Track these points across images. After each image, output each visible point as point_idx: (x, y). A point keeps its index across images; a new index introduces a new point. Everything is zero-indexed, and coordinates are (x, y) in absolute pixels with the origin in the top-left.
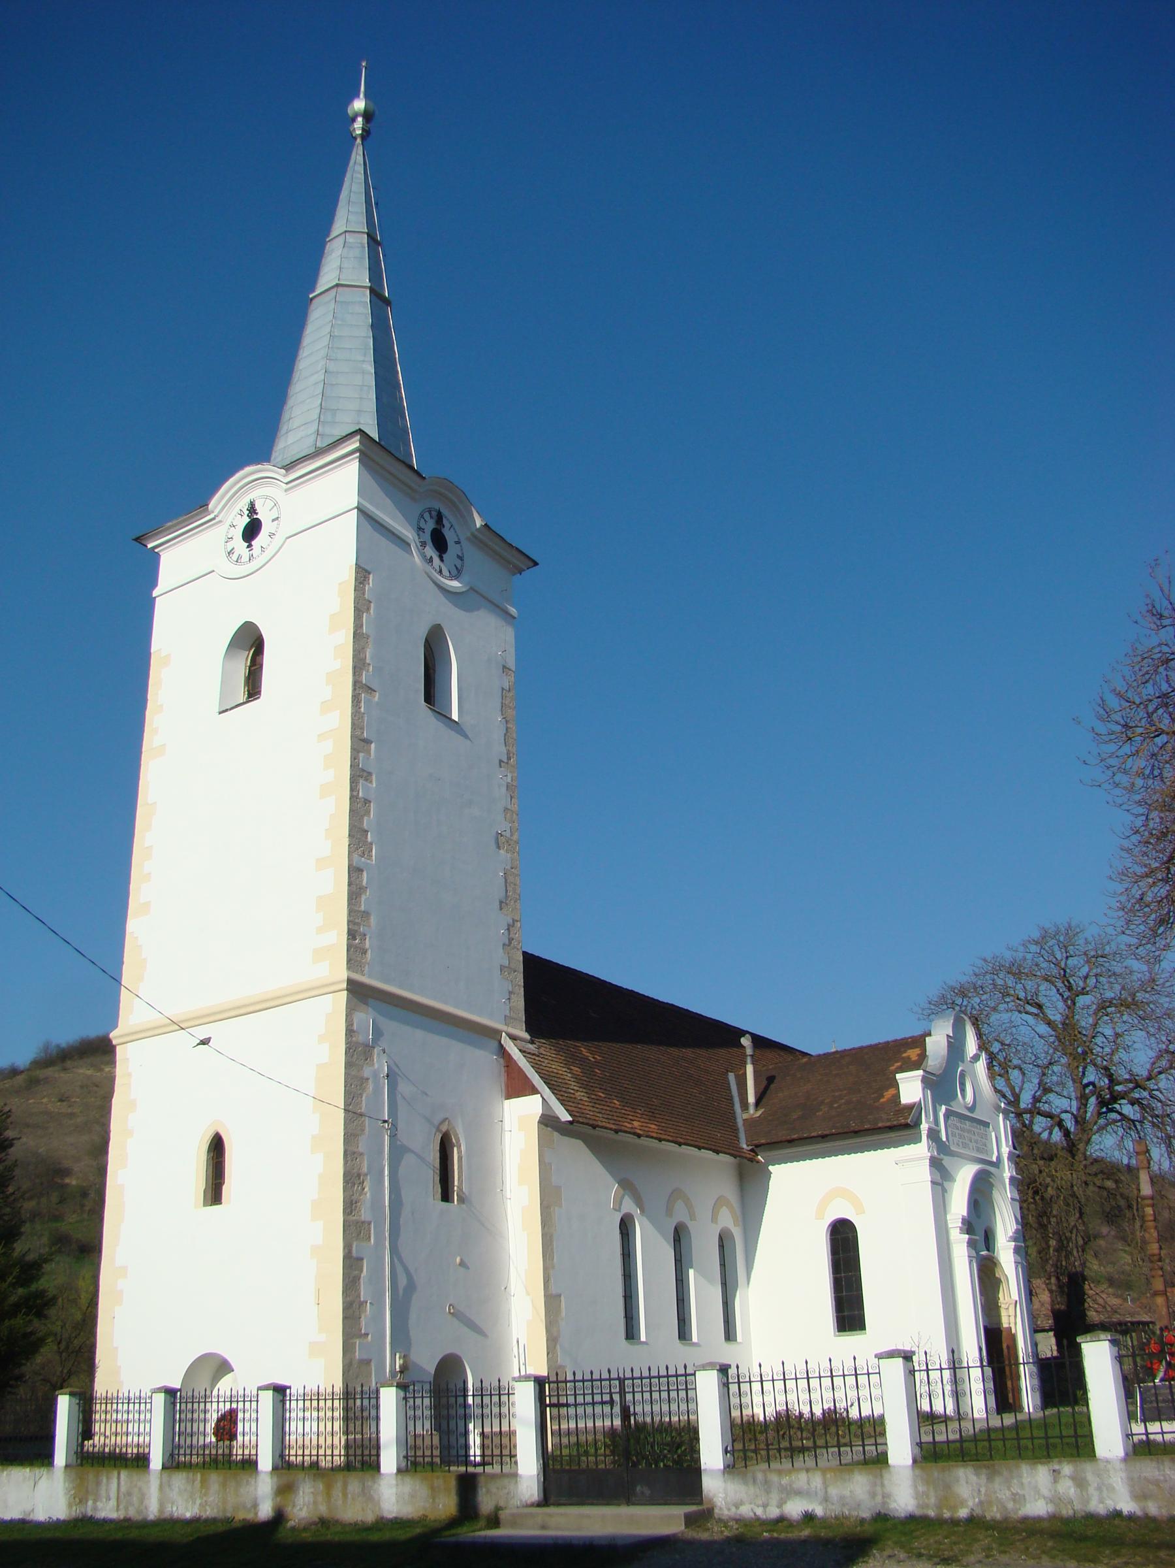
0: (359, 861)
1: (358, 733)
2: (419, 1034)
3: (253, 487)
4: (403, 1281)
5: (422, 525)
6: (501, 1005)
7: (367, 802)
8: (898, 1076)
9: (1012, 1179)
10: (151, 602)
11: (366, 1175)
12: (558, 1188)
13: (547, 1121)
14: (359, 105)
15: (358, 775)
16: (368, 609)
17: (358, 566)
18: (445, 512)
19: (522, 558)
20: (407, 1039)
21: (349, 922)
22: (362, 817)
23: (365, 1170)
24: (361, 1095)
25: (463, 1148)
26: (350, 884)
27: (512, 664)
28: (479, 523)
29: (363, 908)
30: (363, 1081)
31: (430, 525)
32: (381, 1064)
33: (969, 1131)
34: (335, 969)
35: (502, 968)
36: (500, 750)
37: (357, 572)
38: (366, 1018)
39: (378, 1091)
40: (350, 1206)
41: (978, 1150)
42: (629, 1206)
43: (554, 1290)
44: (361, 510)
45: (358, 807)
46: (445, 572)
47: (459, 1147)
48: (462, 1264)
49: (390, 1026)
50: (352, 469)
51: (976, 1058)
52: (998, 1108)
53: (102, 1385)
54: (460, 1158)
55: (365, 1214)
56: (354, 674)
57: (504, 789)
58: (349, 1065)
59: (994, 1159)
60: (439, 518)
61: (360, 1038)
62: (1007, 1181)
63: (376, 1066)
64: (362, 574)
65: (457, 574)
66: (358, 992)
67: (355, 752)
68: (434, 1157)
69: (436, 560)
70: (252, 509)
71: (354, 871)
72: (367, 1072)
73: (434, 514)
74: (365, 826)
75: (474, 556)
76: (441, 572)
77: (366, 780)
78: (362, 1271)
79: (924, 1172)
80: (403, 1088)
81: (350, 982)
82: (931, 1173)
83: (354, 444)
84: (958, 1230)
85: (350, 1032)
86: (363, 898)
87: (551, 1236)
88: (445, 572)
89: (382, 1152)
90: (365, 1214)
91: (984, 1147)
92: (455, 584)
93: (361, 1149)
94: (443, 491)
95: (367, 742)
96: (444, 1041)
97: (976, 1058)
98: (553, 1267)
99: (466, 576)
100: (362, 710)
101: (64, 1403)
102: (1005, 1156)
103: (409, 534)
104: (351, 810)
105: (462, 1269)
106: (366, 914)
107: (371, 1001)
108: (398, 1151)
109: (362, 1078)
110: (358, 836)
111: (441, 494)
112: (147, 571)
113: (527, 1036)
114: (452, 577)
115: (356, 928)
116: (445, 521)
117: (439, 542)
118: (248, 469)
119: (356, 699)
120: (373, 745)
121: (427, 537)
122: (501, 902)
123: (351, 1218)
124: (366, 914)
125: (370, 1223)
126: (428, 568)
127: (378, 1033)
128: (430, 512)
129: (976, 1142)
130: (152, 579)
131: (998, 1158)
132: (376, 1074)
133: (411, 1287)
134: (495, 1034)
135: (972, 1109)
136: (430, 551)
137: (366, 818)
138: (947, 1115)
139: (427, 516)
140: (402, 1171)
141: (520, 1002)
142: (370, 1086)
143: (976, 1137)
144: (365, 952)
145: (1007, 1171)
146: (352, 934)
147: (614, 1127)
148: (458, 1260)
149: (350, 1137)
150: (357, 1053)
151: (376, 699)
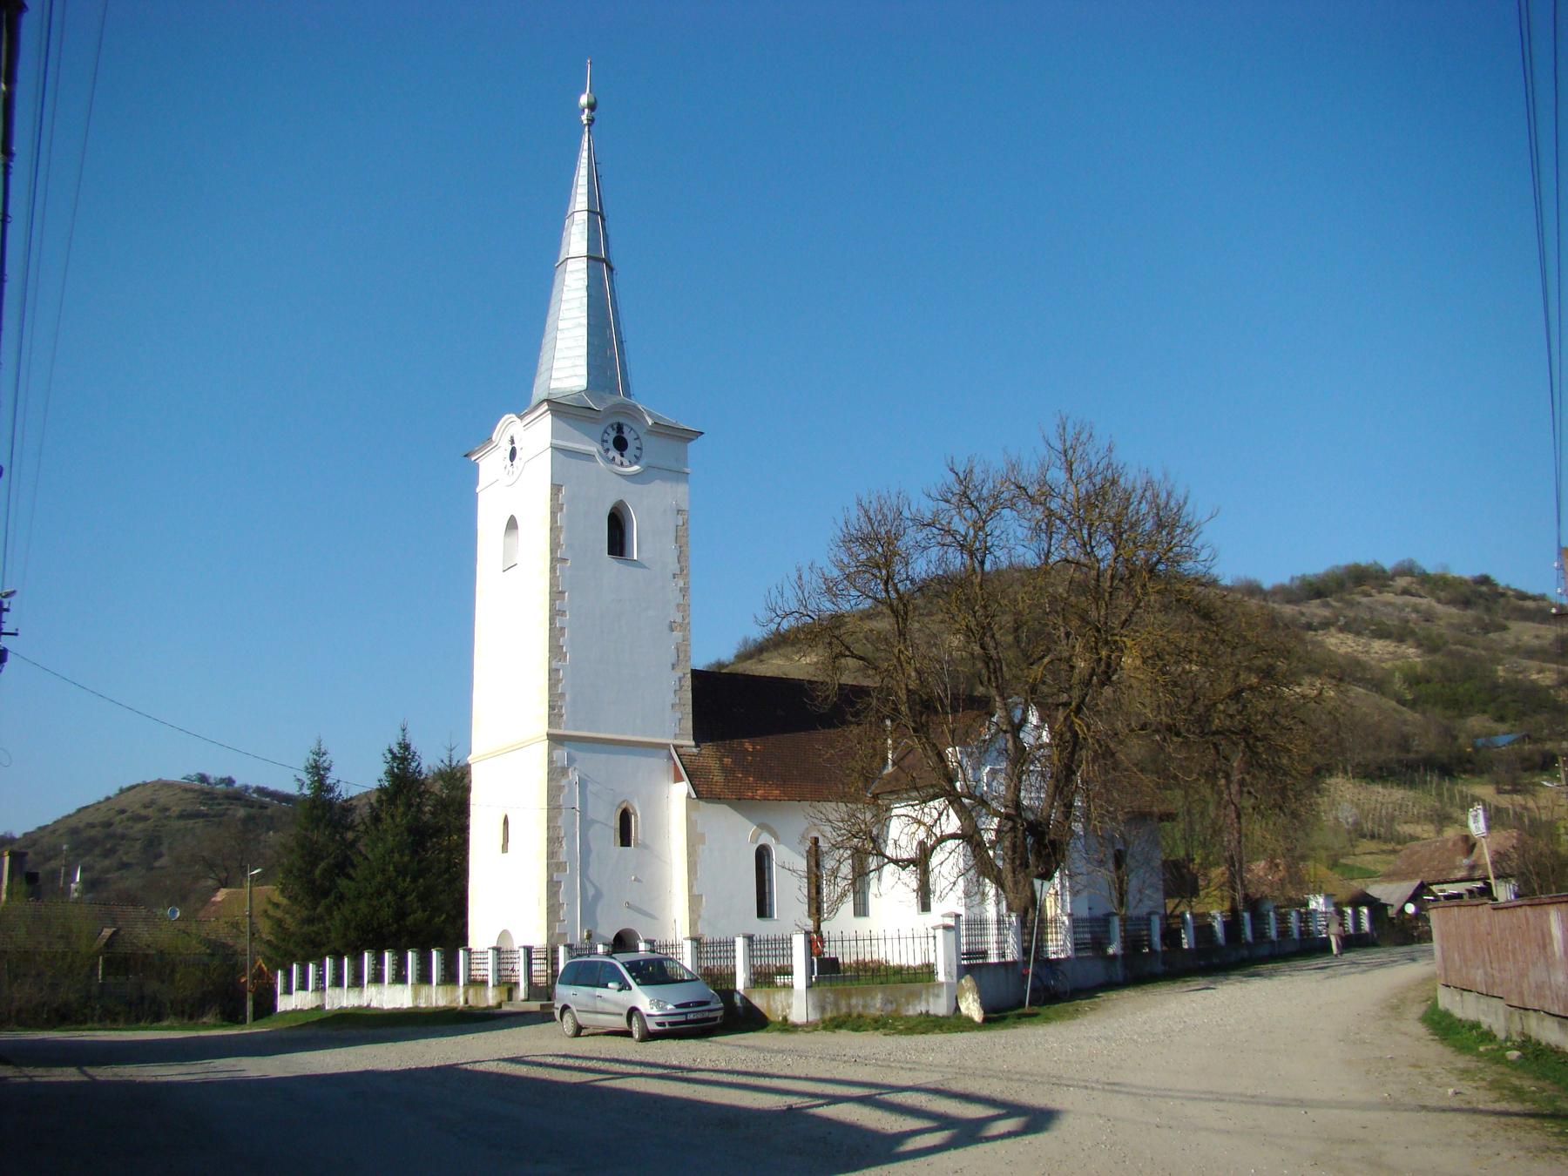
2: (603, 757)
3: (509, 427)
4: (591, 892)
7: (562, 629)
10: (475, 497)
12: (703, 835)
13: (689, 796)
14: (584, 100)
15: (555, 613)
17: (553, 485)
20: (592, 762)
30: (561, 788)
31: (613, 434)
32: (574, 776)
34: (543, 728)
35: (673, 706)
38: (562, 754)
39: (571, 791)
40: (551, 854)
42: (765, 839)
43: (696, 891)
44: (554, 448)
45: (555, 634)
46: (626, 462)
49: (579, 755)
50: (548, 418)
53: (471, 944)
55: (562, 858)
60: (620, 428)
64: (556, 488)
65: (637, 459)
66: (555, 740)
67: (552, 601)
68: (615, 822)
69: (618, 458)
70: (512, 442)
71: (553, 672)
72: (564, 782)
75: (650, 443)
80: (591, 788)
83: (545, 407)
85: (551, 762)
88: (626, 462)
89: (574, 824)
90: (562, 858)
92: (636, 468)
95: (563, 593)
96: (623, 757)
99: (643, 461)
101: (461, 952)
103: (593, 448)
106: (563, 695)
108: (586, 824)
110: (555, 650)
112: (471, 476)
114: (631, 464)
116: (625, 429)
117: (621, 444)
119: (553, 569)
121: (610, 445)
124: (563, 695)
127: (571, 760)
130: (474, 480)
132: (570, 783)
133: (598, 895)
134: (665, 746)
136: (614, 453)
141: (689, 724)
146: (551, 708)
149: (551, 820)
150: (556, 773)
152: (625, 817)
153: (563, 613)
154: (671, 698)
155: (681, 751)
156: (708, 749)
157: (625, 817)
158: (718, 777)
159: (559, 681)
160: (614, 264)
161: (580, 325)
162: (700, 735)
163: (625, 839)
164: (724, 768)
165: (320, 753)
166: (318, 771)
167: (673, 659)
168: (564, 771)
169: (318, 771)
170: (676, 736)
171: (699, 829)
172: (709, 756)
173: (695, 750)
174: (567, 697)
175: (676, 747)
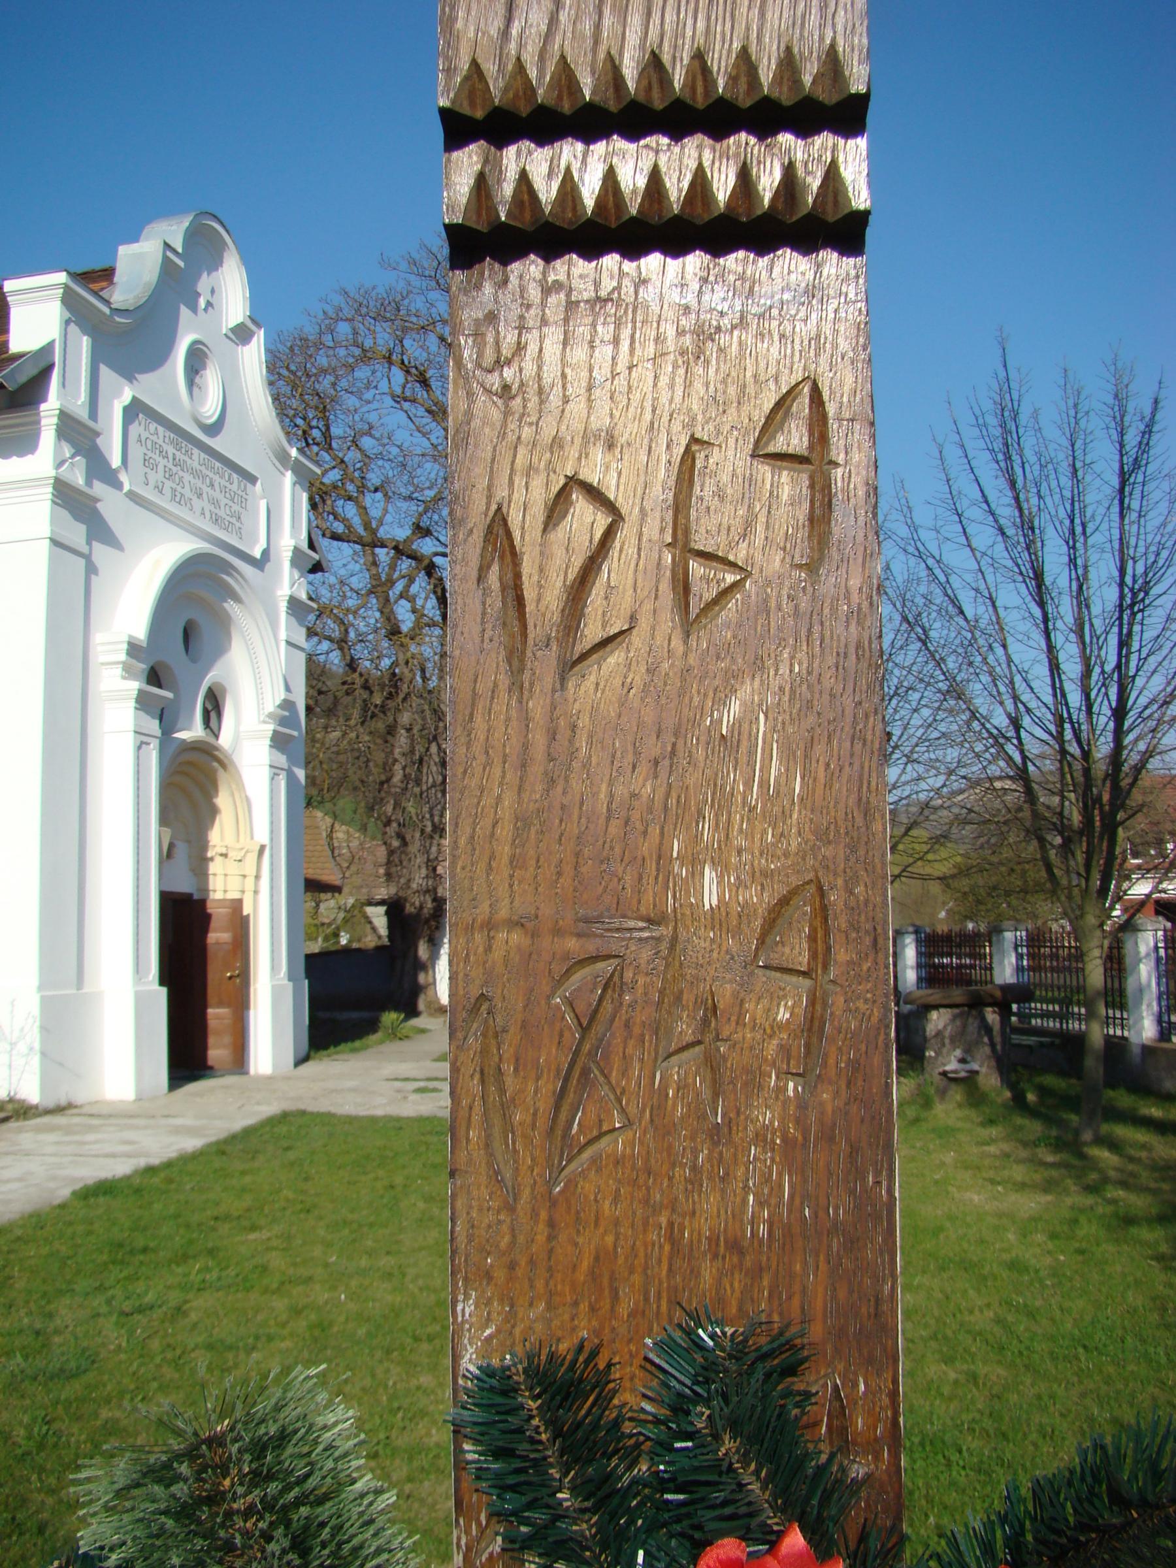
8: (9, 286)
9: (293, 602)
33: (195, 473)
41: (216, 520)
51: (241, 334)
52: (283, 458)
59: (257, 554)
62: (283, 606)
79: (37, 515)
82: (54, 520)
84: (118, 671)
91: (236, 521)
97: (241, 334)
102: (287, 555)
129: (215, 502)
131: (266, 553)
135: (214, 429)
138: (135, 410)
143: (217, 494)
145: (287, 583)
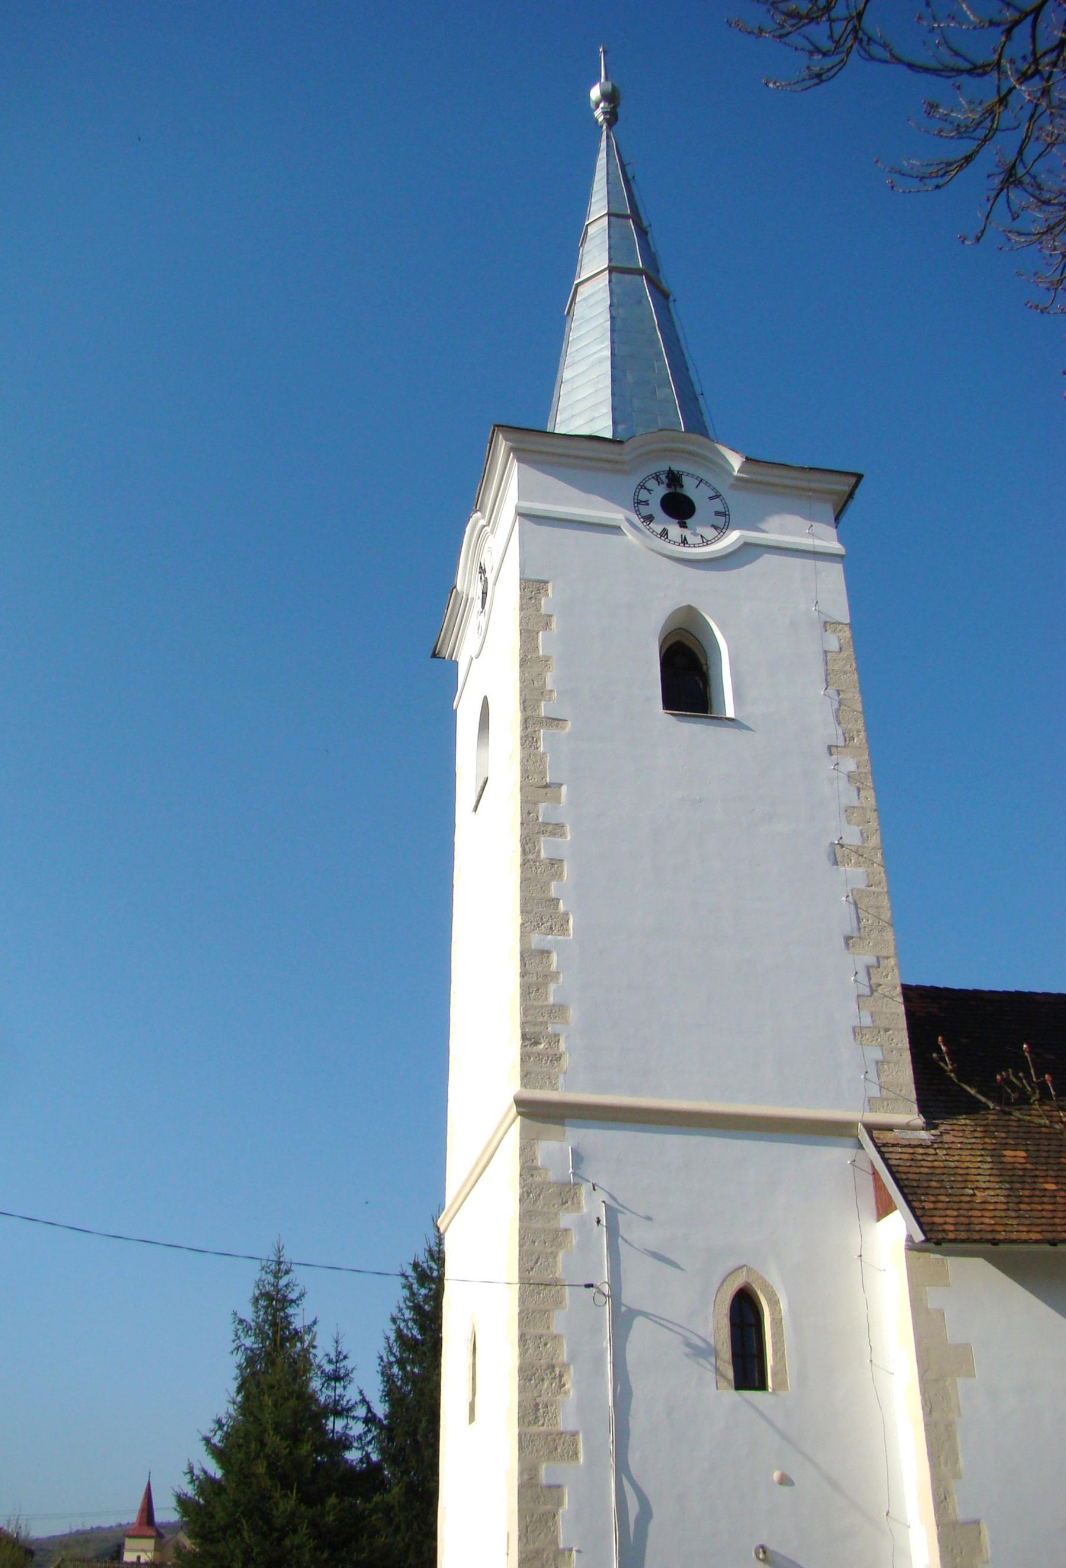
0: (536, 940)
1: (535, 779)
5: (643, 495)
6: (872, 1080)
7: (555, 863)
11: (566, 1366)
13: (912, 1246)
16: (547, 625)
18: (675, 468)
19: (818, 476)
21: (523, 1025)
22: (547, 884)
23: (564, 1356)
24: (554, 1255)
25: (783, 1305)
26: (523, 975)
27: (843, 614)
28: (735, 461)
29: (551, 1000)
30: (558, 1236)
32: (592, 1205)
35: (858, 1031)
36: (833, 733)
37: (523, 589)
38: (557, 1148)
43: (960, 1512)
47: (774, 1303)
48: (785, 1480)
54: (777, 1323)
55: (567, 1419)
56: (524, 709)
57: (843, 783)
58: (526, 1215)
60: (674, 479)
61: (552, 1176)
63: (585, 1210)
68: (715, 1327)
72: (566, 1219)
73: (663, 477)
74: (553, 894)
76: (684, 541)
77: (553, 834)
78: (559, 1503)
81: (519, 1103)
85: (528, 1169)
86: (552, 987)
87: (949, 1427)
88: (691, 539)
90: (567, 1419)
93: (555, 1329)
94: (666, 445)
98: (957, 1475)
100: (541, 749)
103: (617, 515)
104: (524, 880)
105: (786, 1489)
106: (558, 1011)
107: (567, 1121)
109: (556, 1231)
111: (666, 450)
113: (919, 1120)
115: (537, 1029)
116: (686, 481)
117: (679, 508)
118: (468, 529)
120: (564, 789)
122: (848, 939)
123: (535, 1429)
124: (558, 1011)
125: (574, 1434)
126: (660, 544)
128: (657, 477)
137: (553, 884)
139: (652, 484)
140: (631, 1356)
142: (574, 1239)
144: (558, 1058)
147: (1039, 1236)
148: (776, 1475)
151: (567, 730)
152: (745, 1312)
153: (557, 829)
154: (848, 1014)
155: (889, 1137)
156: (960, 1131)
157: (745, 1312)
158: (988, 1192)
159: (550, 976)
160: (668, 281)
161: (601, 361)
162: (936, 1097)
163: (748, 1368)
164: (1004, 1172)
165: (279, 1269)
166: (275, 1303)
167: (848, 926)
168: (567, 1194)
169: (275, 1303)
170: (872, 1103)
171: (953, 1334)
172: (962, 1146)
173: (925, 1135)
174: (572, 1013)
175: (870, 1128)
